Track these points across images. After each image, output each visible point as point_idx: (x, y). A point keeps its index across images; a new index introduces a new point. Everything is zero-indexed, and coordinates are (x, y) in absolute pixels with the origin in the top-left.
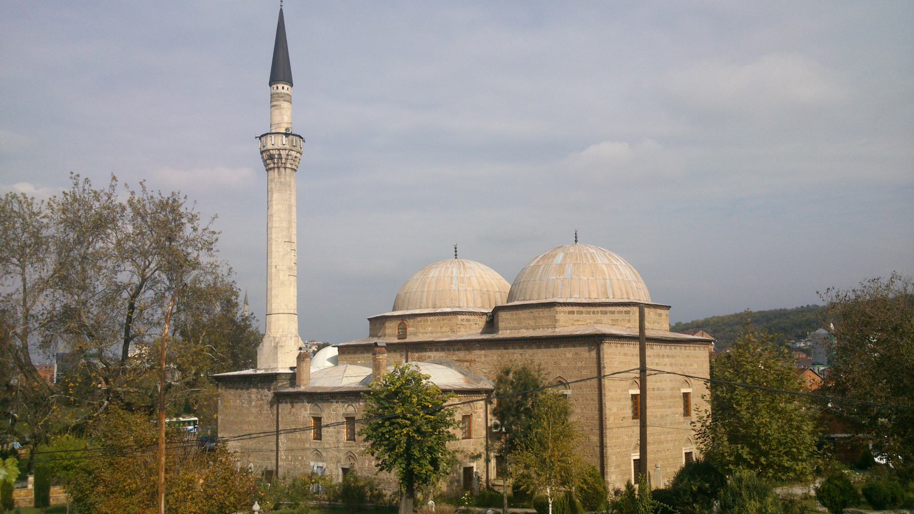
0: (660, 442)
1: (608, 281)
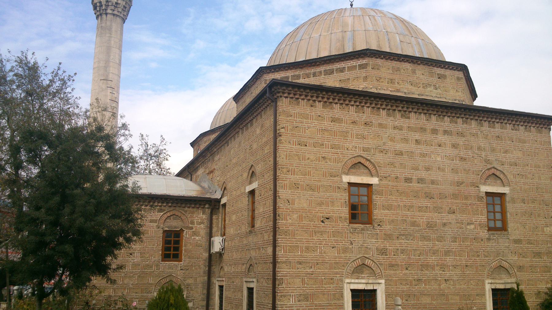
0: (425, 266)
1: (349, 35)
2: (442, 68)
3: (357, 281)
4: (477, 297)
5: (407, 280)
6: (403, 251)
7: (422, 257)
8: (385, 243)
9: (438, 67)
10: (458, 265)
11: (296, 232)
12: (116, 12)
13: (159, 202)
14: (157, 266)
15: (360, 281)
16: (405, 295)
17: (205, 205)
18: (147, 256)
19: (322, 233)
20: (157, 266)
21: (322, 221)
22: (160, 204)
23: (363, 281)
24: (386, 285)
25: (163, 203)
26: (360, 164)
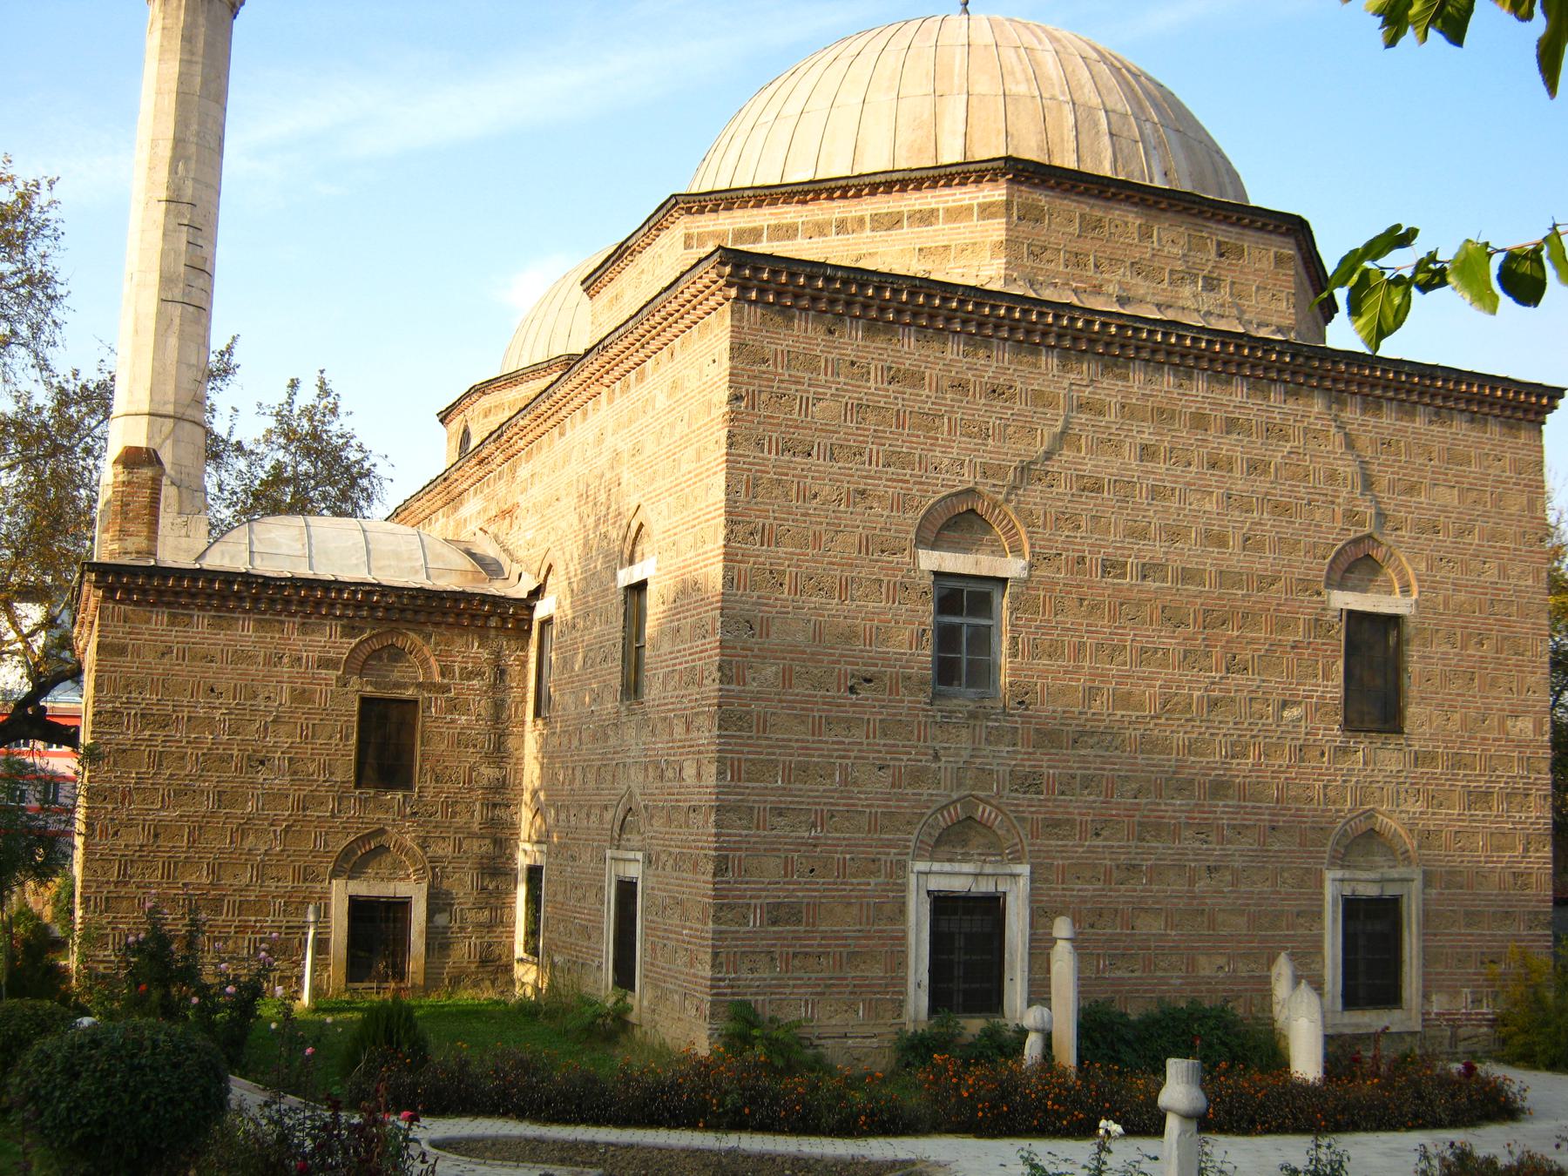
2: (1232, 224)
3: (947, 867)
4: (1301, 920)
5: (1095, 866)
6: (1087, 782)
7: (1144, 801)
8: (1038, 756)
9: (1219, 222)
10: (1247, 827)
11: (771, 720)
15: (957, 867)
16: (1089, 910)
19: (849, 724)
21: (852, 690)
23: (968, 868)
24: (1032, 881)
26: (972, 516)
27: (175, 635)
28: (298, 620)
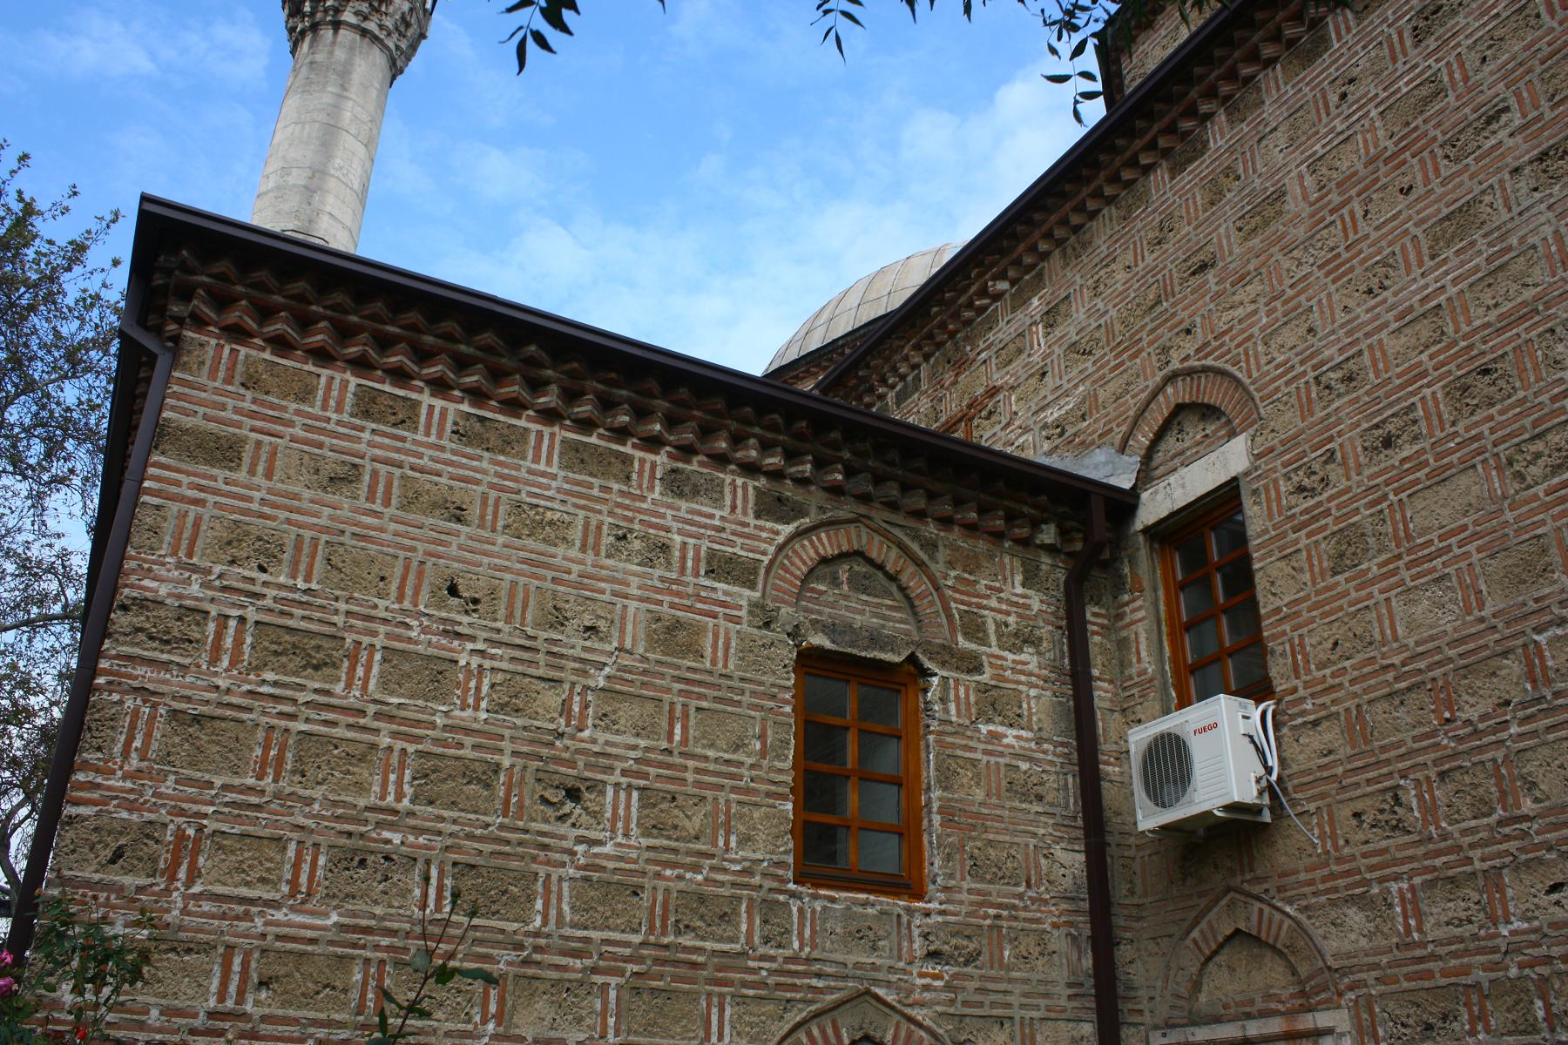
12: (371, 26)
13: (766, 447)
14: (770, 909)
17: (1036, 525)
18: (694, 825)
20: (770, 909)
22: (774, 461)
25: (791, 456)
27: (370, 440)
28: (661, 459)
